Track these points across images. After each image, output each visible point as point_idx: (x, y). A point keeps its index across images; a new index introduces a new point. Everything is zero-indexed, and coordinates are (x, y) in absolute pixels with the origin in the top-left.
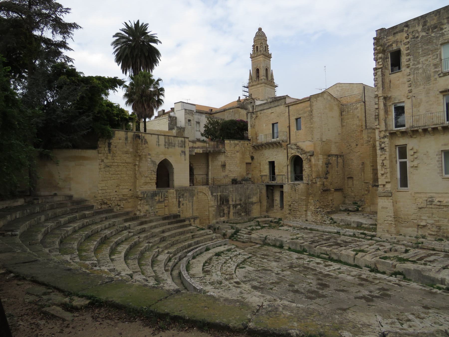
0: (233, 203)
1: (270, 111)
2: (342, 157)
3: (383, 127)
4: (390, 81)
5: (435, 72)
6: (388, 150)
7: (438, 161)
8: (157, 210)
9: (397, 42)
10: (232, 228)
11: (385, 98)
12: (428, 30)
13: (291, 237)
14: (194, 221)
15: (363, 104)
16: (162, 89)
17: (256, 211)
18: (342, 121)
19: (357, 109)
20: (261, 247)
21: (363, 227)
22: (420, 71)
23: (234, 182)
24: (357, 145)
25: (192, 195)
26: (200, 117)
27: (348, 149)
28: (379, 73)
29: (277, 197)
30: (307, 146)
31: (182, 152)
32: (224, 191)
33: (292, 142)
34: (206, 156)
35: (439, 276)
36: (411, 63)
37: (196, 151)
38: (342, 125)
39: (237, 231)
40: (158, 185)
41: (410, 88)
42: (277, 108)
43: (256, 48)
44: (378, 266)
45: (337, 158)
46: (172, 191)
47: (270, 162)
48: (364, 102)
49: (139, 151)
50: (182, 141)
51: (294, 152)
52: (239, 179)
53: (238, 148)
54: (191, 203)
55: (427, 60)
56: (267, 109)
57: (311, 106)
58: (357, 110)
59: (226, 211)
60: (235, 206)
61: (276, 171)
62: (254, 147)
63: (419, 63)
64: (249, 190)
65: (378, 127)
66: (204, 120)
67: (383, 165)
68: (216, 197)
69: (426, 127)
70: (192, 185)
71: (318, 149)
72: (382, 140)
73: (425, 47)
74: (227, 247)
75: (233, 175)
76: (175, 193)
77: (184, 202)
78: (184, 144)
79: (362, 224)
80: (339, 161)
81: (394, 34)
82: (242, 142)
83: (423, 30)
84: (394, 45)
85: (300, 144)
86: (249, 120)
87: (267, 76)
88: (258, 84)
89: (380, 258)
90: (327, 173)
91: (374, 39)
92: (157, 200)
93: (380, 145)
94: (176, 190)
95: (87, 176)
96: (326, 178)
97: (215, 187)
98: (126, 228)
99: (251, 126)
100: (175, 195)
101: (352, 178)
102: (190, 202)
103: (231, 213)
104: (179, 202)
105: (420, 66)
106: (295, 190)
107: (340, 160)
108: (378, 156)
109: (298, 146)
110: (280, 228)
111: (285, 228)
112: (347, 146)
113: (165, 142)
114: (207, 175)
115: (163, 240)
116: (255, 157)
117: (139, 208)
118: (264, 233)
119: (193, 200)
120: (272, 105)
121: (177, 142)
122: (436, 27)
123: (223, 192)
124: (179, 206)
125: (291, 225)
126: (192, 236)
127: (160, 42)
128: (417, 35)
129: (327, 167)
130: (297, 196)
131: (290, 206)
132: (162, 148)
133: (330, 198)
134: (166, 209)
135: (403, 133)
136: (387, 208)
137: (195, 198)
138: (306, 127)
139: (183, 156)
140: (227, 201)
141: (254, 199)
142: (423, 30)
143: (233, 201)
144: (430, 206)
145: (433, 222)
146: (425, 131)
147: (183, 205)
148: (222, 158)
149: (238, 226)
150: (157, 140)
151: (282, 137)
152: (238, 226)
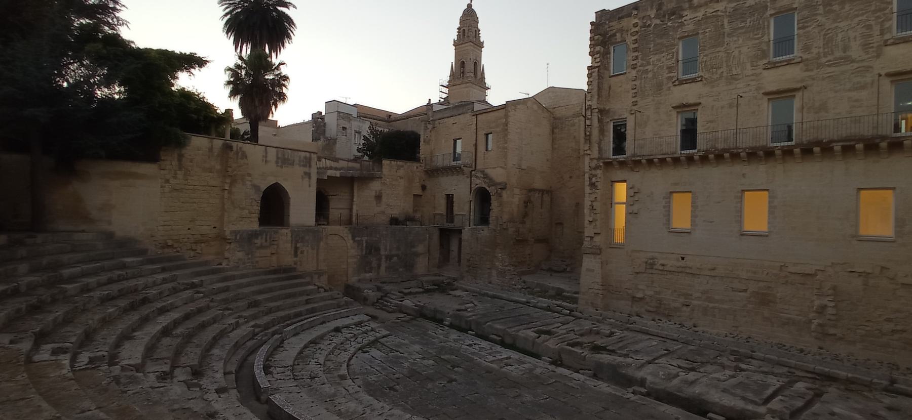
1: (452, 120)
3: (595, 153)
4: (610, 88)
5: (670, 78)
6: (599, 187)
7: (664, 207)
8: (257, 259)
9: (621, 30)
10: (379, 289)
11: (601, 111)
12: (664, 16)
13: (459, 307)
14: (319, 278)
16: (286, 78)
17: (421, 266)
20: (412, 319)
21: (564, 296)
22: (650, 75)
23: (394, 221)
24: (571, 177)
26: (361, 124)
28: (595, 74)
29: (454, 247)
30: (498, 175)
31: (305, 173)
33: (480, 166)
34: (349, 182)
35: (640, 374)
36: (639, 62)
37: (330, 173)
39: (386, 294)
41: (634, 99)
43: (462, 32)
44: (563, 356)
46: (284, 231)
47: (448, 195)
49: (229, 169)
50: (305, 158)
51: (479, 182)
52: (401, 219)
53: (401, 172)
55: (659, 60)
57: (506, 116)
59: (374, 264)
60: (389, 258)
61: (455, 208)
62: (427, 172)
63: (649, 64)
65: (588, 152)
66: (365, 128)
67: (592, 208)
68: (359, 243)
69: (652, 157)
72: (593, 172)
73: (659, 41)
74: (357, 319)
75: (395, 212)
76: (290, 235)
79: (563, 291)
81: (620, 18)
82: (409, 164)
83: (657, 16)
84: (618, 35)
85: (488, 171)
86: (422, 133)
87: (475, 73)
88: (462, 83)
89: (568, 345)
90: (525, 215)
91: (592, 23)
92: (258, 245)
93: (590, 179)
94: (292, 232)
95: (135, 202)
96: (523, 222)
97: (357, 227)
98: (193, 286)
100: (289, 238)
101: (561, 224)
102: (313, 249)
103: (383, 268)
104: (296, 249)
105: (650, 68)
107: (547, 198)
108: (587, 195)
110: (451, 292)
111: (458, 293)
113: (278, 158)
114: (351, 209)
115: (255, 304)
116: (428, 187)
117: (227, 255)
118: (424, 300)
122: (673, 14)
124: (296, 255)
125: (468, 288)
126: (307, 300)
127: (294, 7)
128: (649, 22)
129: (526, 207)
134: (274, 258)
135: (622, 164)
136: (593, 271)
137: (322, 244)
140: (378, 250)
141: (420, 248)
142: (657, 16)
143: (386, 250)
144: (650, 271)
145: (652, 293)
146: (650, 162)
147: (302, 252)
148: (376, 186)
149: (387, 288)
151: (466, 160)
152: (387, 288)
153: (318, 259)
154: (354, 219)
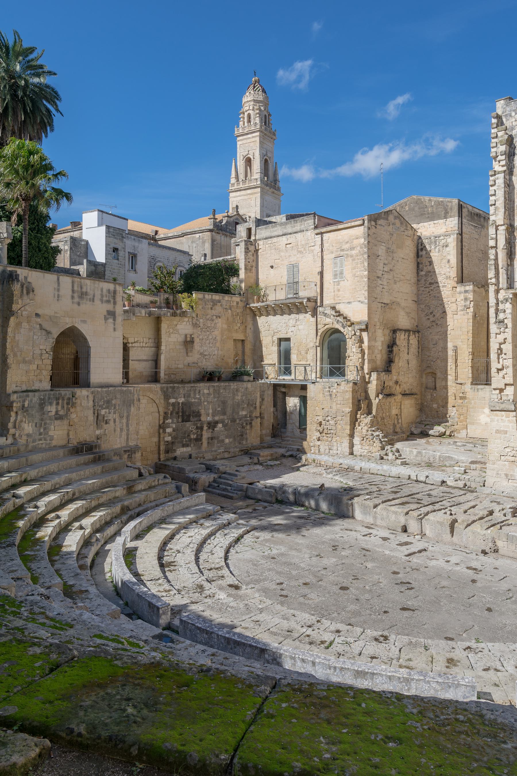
0: (209, 419)
2: (417, 335)
15: (460, 237)
18: (418, 267)
19: (447, 246)
25: (128, 403)
27: (429, 319)
32: (192, 395)
33: (326, 302)
38: (418, 273)
40: (56, 382)
42: (299, 235)
45: (409, 336)
48: (461, 234)
50: (109, 291)
51: (329, 321)
53: (218, 309)
54: (124, 421)
56: (278, 236)
58: (448, 249)
64: (240, 394)
70: (125, 381)
71: (376, 319)
76: (91, 398)
77: (111, 417)
78: (114, 298)
80: (411, 342)
99: (246, 269)
100: (91, 403)
102: (121, 417)
106: (331, 395)
109: (339, 312)
112: (427, 315)
113: (73, 291)
119: (129, 413)
120: (289, 229)
121: (98, 293)
123: (189, 396)
130: (334, 407)
131: (320, 425)
132: (66, 302)
133: (394, 411)
138: (354, 276)
139: (111, 320)
150: (56, 286)
153: (128, 430)
154: (162, 375)
